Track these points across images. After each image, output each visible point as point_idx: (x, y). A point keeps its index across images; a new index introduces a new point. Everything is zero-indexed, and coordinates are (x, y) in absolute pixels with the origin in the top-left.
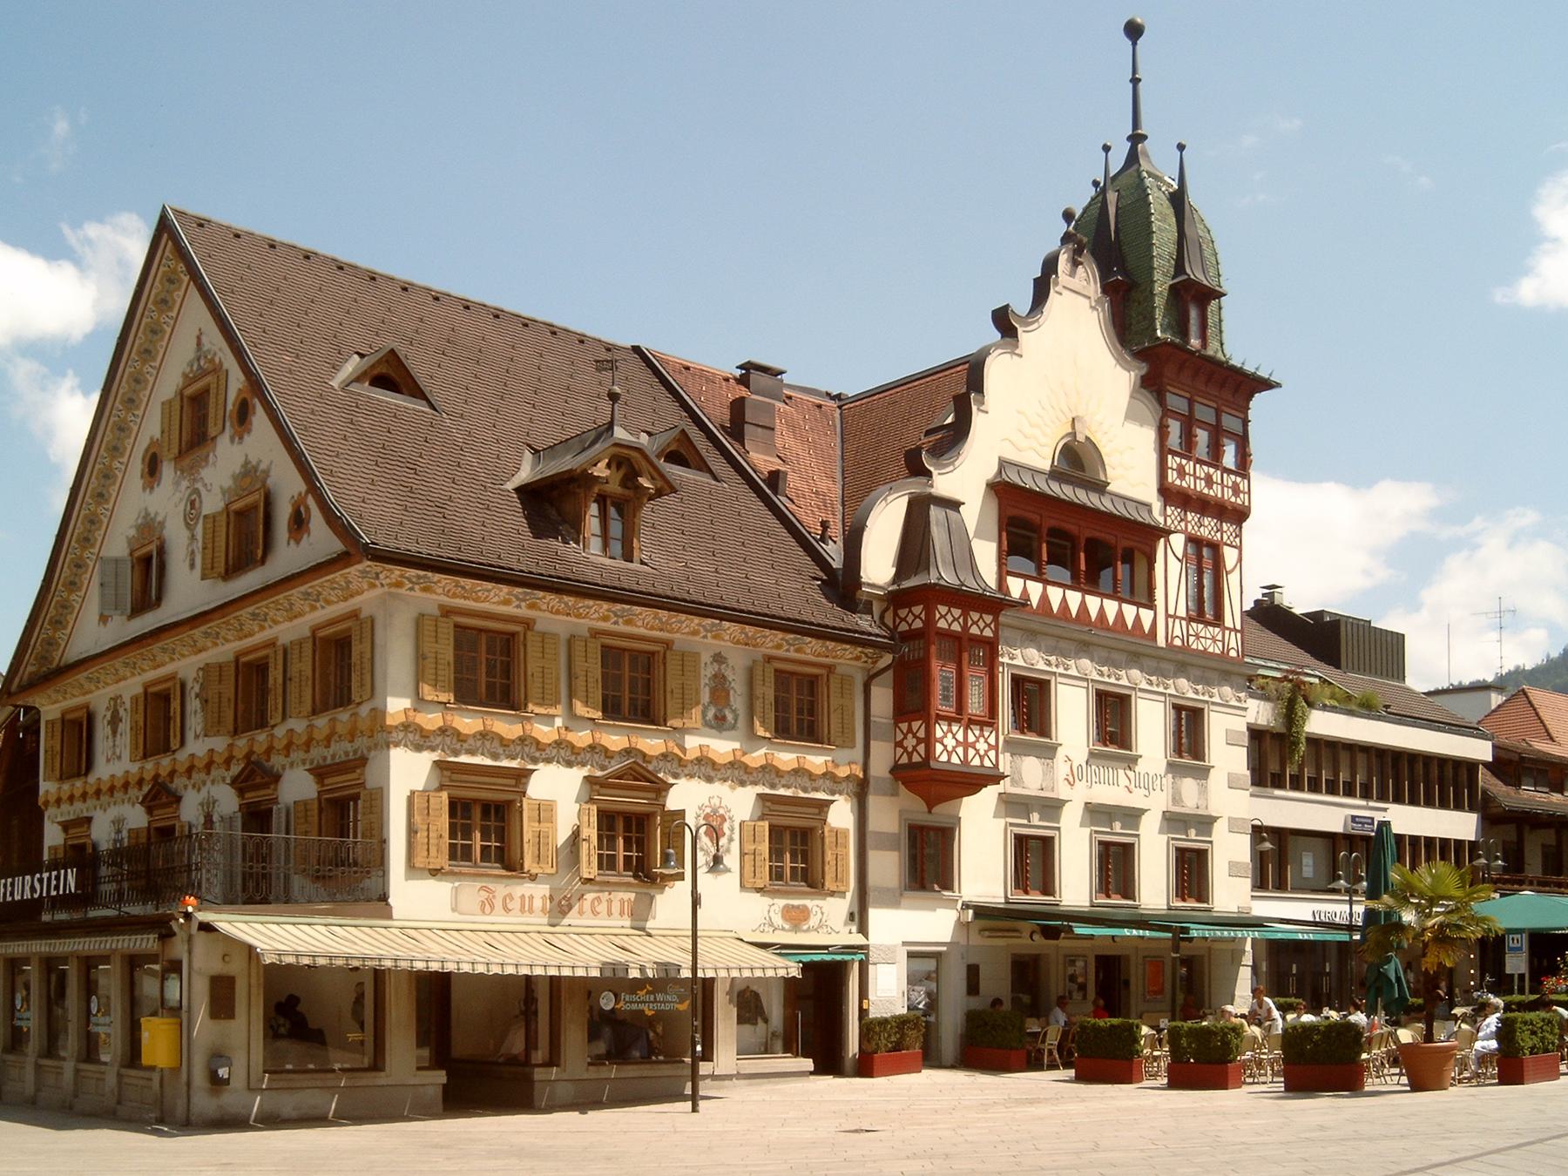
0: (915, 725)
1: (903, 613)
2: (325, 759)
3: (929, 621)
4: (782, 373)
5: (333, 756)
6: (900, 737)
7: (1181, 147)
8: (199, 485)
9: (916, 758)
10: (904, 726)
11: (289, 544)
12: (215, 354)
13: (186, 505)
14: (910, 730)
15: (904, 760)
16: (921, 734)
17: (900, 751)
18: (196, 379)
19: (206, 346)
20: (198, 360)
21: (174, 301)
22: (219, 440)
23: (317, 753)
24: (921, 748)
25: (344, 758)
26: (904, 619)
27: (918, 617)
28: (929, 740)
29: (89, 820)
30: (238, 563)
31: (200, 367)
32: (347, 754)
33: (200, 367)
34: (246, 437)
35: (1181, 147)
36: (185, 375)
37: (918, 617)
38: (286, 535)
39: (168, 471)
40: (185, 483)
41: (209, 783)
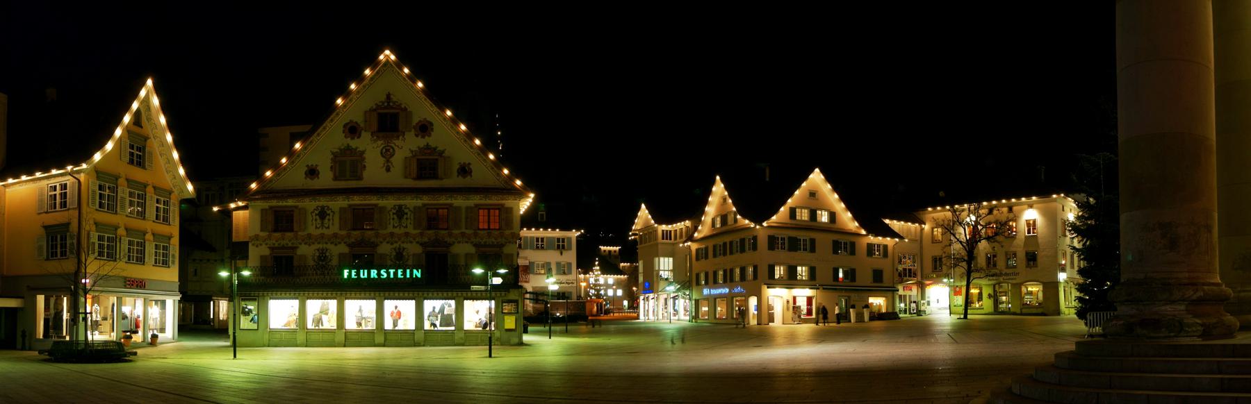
5: (485, 242)
8: (393, 145)
11: (458, 176)
12: (401, 104)
13: (382, 150)
18: (386, 108)
20: (388, 103)
29: (297, 248)
30: (420, 177)
31: (388, 104)
32: (493, 242)
33: (388, 104)
34: (427, 137)
36: (376, 104)
38: (456, 174)
39: (366, 136)
40: (380, 142)
41: (399, 243)
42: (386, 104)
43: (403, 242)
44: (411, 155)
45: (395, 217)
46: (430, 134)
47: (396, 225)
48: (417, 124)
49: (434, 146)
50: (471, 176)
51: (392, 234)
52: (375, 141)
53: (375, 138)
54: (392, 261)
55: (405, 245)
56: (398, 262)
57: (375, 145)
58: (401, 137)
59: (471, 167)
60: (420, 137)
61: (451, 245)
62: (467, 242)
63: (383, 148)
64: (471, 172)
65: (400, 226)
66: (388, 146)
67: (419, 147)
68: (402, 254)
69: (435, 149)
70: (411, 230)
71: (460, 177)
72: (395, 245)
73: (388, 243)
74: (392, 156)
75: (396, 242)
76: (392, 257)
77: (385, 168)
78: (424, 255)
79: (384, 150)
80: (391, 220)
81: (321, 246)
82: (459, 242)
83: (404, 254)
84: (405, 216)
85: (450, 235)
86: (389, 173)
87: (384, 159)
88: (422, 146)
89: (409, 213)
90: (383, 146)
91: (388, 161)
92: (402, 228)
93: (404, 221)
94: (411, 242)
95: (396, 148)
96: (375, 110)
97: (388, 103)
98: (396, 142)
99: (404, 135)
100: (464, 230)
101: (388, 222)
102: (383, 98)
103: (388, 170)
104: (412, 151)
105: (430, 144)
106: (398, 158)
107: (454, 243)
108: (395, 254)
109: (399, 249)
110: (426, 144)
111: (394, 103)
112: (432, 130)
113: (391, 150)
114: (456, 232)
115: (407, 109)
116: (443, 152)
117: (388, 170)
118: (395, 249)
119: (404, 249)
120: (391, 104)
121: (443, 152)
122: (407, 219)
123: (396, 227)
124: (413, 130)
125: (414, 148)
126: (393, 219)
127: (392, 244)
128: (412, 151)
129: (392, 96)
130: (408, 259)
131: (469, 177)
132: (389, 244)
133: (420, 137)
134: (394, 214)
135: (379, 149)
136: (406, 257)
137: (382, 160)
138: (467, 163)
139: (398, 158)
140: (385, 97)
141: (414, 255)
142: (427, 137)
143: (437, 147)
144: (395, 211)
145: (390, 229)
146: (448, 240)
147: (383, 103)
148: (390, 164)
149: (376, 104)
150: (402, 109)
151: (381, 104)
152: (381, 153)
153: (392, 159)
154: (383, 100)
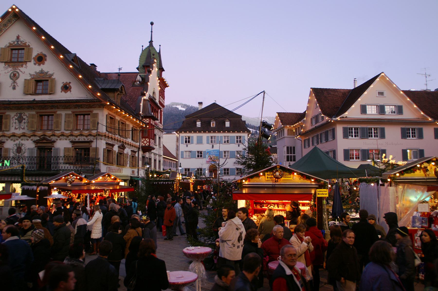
0: (147, 139)
1: (144, 119)
2: (75, 139)
3: (150, 121)
4: (97, 66)
5: (79, 139)
6: (143, 141)
7: (160, 46)
8: (18, 71)
9: (146, 145)
10: (144, 139)
11: (61, 92)
12: (26, 43)
13: (11, 75)
14: (145, 140)
15: (144, 145)
16: (148, 141)
17: (143, 143)
18: (15, 46)
19: (21, 39)
20: (18, 42)
21: (8, 26)
22: (28, 64)
23: (72, 138)
24: (148, 143)
25: (83, 140)
26: (144, 121)
27: (148, 121)
28: (149, 142)
32: (85, 139)
34: (42, 65)
35: (160, 46)
36: (9, 43)
37: (148, 121)
38: (61, 90)
42: (16, 43)
43: (22, 140)
44: (30, 77)
45: (17, 121)
46: (44, 62)
47: (17, 128)
48: (36, 56)
49: (46, 71)
50: (71, 91)
51: (14, 135)
52: (6, 68)
53: (7, 66)
54: (14, 153)
55: (23, 142)
56: (18, 154)
57: (6, 71)
58: (24, 66)
59: (71, 85)
60: (37, 64)
61: (54, 142)
62: (66, 139)
63: (12, 73)
64: (71, 88)
65: (20, 127)
66: (15, 72)
67: (36, 72)
68: (21, 148)
69: (47, 73)
70: (25, 131)
71: (63, 92)
72: (17, 142)
73: (12, 140)
74: (18, 78)
75: (17, 140)
76: (14, 150)
77: (12, 87)
78: (36, 149)
79: (12, 75)
80: (14, 124)
81: (17, 142)
82: (60, 139)
83: (22, 148)
84: (24, 121)
85: (54, 135)
86: (15, 91)
87: (12, 81)
88: (38, 71)
89: (26, 119)
90: (12, 71)
91: (15, 82)
92: (21, 129)
93: (22, 124)
94: (28, 140)
95: (20, 73)
96: (8, 47)
97: (18, 42)
98: (21, 69)
99: (26, 64)
100: (63, 130)
101: (12, 125)
102: (14, 39)
103: (14, 88)
104: (31, 75)
105: (43, 70)
106: (20, 82)
107: (57, 140)
108: (16, 148)
109: (19, 144)
110: (41, 70)
111: (21, 42)
112: (46, 60)
113: (17, 75)
114: (57, 133)
115: (29, 46)
116: (52, 75)
117: (14, 88)
118: (16, 145)
119: (22, 145)
120: (19, 43)
121: (52, 75)
122: (25, 123)
123: (17, 129)
124: (33, 60)
125: (33, 73)
126: (15, 123)
127: (14, 141)
128: (31, 75)
129: (20, 38)
130: (25, 152)
131: (69, 92)
132: (12, 142)
133: (37, 64)
134: (16, 119)
135: (9, 74)
136: (24, 150)
137: (10, 81)
138: (68, 82)
139: (20, 82)
140: (16, 38)
141: (28, 149)
142: (42, 65)
143: (48, 72)
144: (16, 118)
145: (13, 130)
146: (53, 138)
147: (14, 42)
148: (16, 84)
149: (9, 43)
150: (26, 46)
151: (12, 43)
152: (10, 77)
153: (18, 81)
154: (14, 40)
